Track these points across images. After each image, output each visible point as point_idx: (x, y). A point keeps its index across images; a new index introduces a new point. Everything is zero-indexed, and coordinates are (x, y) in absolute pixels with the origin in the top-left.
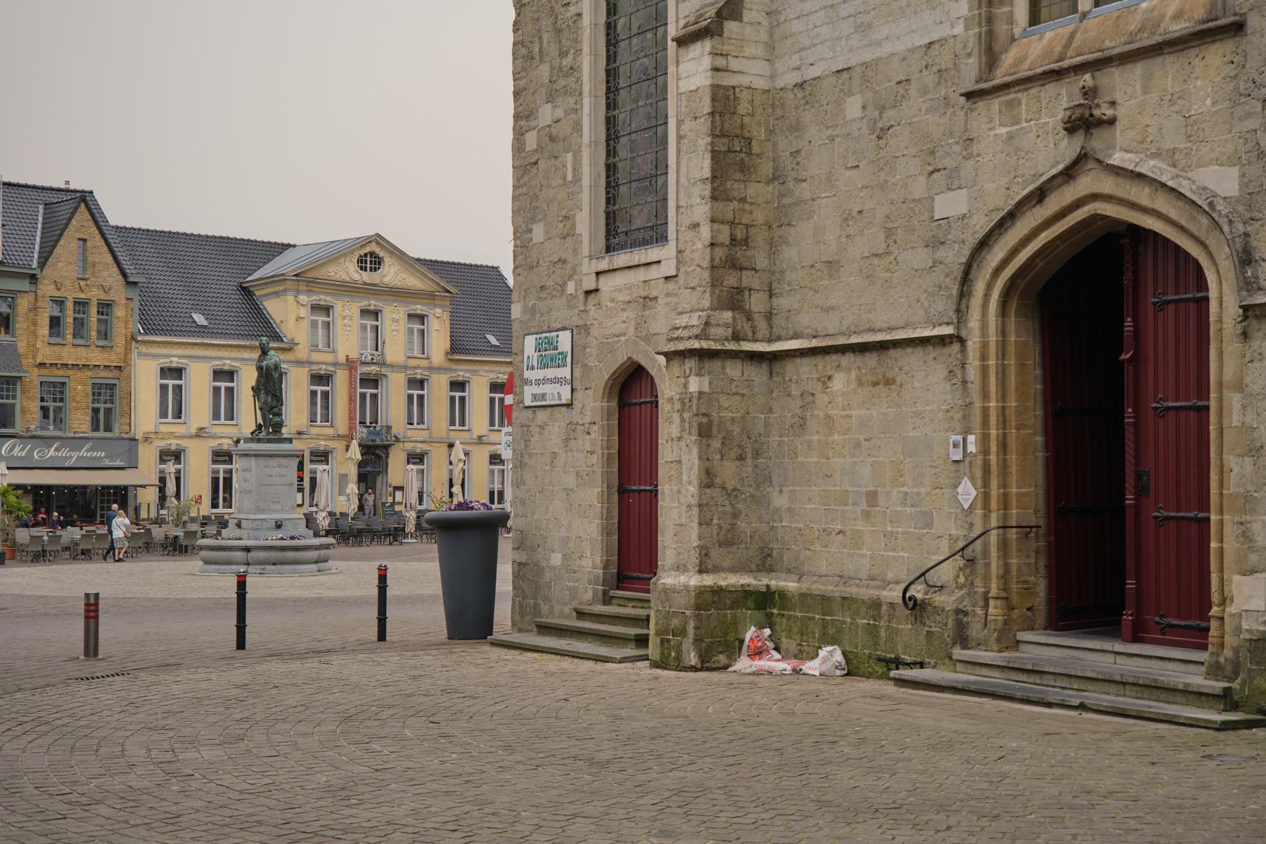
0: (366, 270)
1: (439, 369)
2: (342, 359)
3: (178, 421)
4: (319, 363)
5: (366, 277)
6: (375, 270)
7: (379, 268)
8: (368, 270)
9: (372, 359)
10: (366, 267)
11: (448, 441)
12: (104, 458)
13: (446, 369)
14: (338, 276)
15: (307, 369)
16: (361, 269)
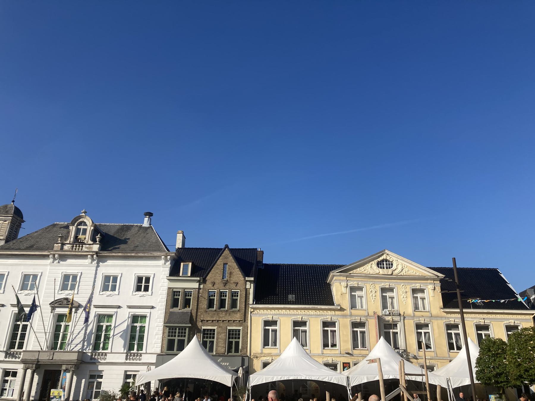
0: (384, 268)
1: (437, 317)
2: (371, 313)
3: (274, 347)
4: (356, 316)
5: (381, 271)
6: (390, 268)
7: (392, 267)
8: (385, 268)
9: (390, 313)
10: (384, 268)
11: (449, 359)
12: (228, 366)
13: (442, 317)
14: (366, 272)
15: (349, 319)
16: (381, 268)
